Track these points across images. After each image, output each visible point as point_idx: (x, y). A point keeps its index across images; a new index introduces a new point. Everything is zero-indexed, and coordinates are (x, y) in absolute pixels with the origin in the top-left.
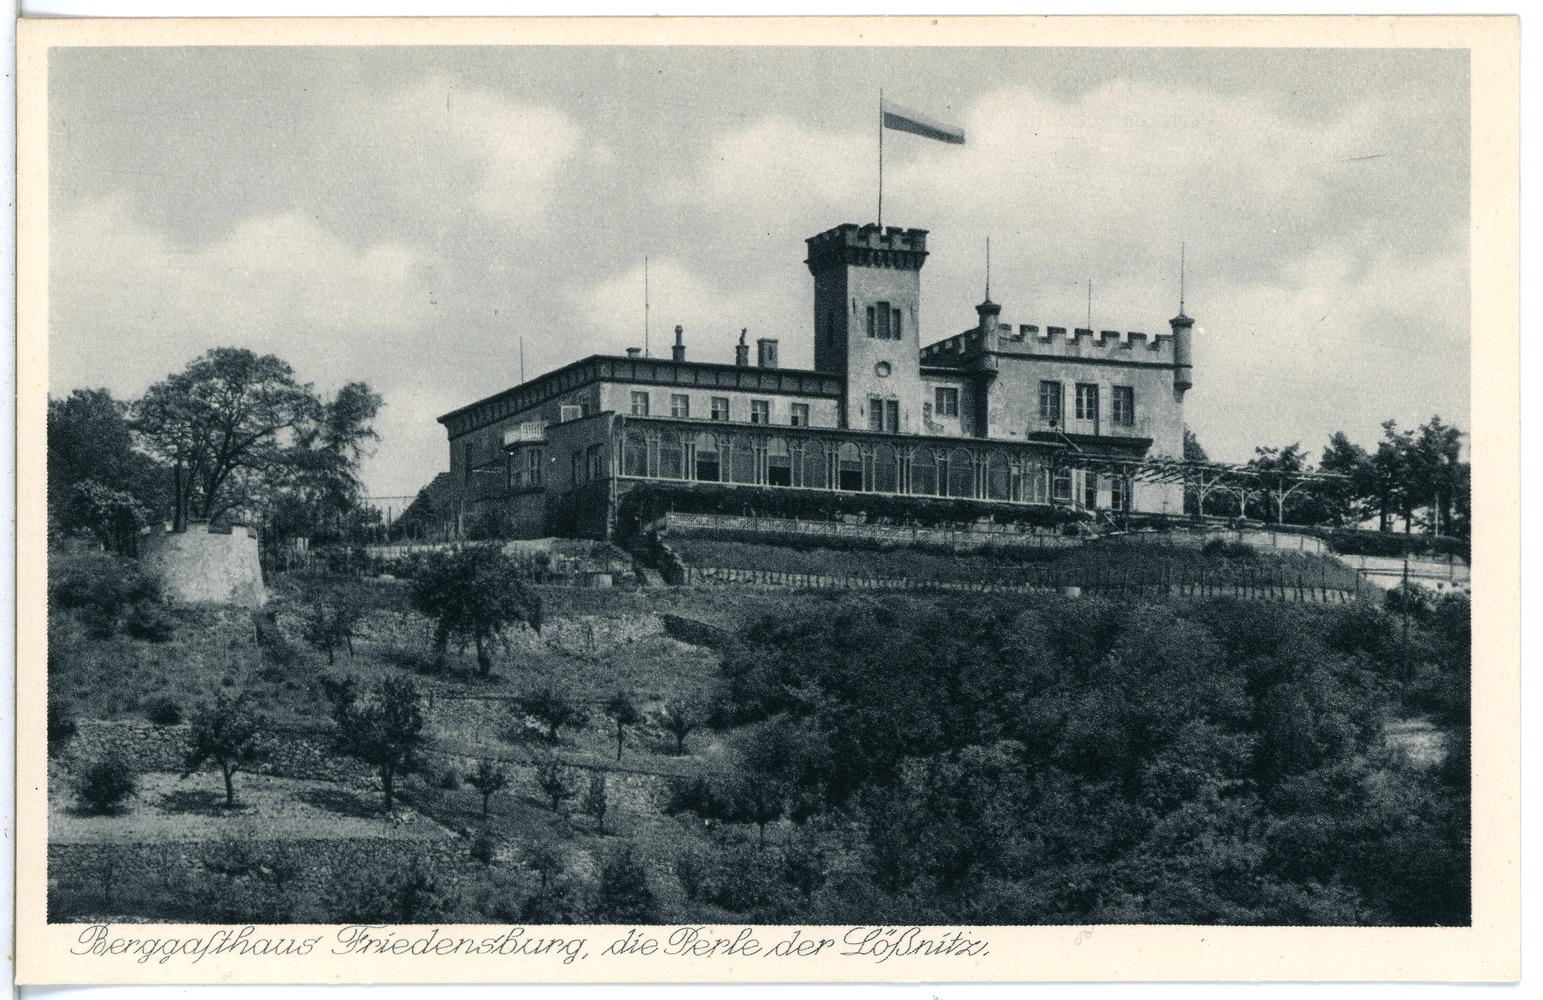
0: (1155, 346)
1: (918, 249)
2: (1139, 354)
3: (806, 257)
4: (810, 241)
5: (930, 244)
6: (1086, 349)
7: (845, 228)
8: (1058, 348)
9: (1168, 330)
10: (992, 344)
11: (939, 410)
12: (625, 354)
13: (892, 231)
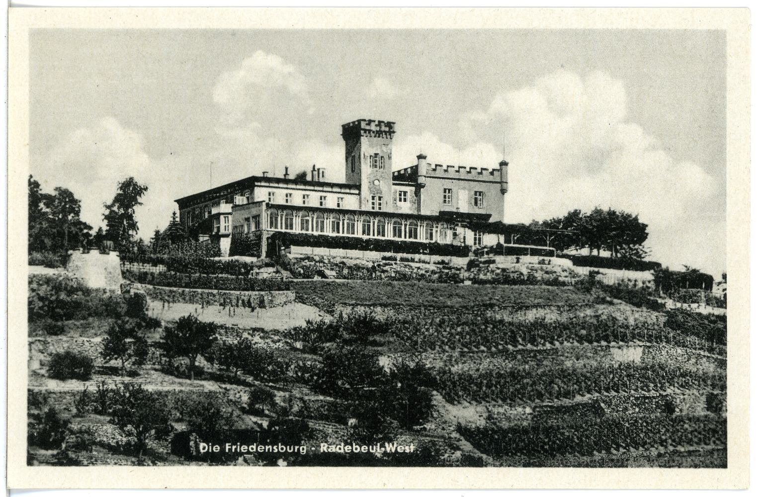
0: (492, 173)
1: (392, 130)
2: (486, 176)
3: (341, 133)
4: (343, 126)
5: (396, 128)
7: (359, 121)
8: (452, 173)
9: (498, 168)
10: (423, 171)
11: (400, 200)
12: (261, 175)
13: (380, 122)
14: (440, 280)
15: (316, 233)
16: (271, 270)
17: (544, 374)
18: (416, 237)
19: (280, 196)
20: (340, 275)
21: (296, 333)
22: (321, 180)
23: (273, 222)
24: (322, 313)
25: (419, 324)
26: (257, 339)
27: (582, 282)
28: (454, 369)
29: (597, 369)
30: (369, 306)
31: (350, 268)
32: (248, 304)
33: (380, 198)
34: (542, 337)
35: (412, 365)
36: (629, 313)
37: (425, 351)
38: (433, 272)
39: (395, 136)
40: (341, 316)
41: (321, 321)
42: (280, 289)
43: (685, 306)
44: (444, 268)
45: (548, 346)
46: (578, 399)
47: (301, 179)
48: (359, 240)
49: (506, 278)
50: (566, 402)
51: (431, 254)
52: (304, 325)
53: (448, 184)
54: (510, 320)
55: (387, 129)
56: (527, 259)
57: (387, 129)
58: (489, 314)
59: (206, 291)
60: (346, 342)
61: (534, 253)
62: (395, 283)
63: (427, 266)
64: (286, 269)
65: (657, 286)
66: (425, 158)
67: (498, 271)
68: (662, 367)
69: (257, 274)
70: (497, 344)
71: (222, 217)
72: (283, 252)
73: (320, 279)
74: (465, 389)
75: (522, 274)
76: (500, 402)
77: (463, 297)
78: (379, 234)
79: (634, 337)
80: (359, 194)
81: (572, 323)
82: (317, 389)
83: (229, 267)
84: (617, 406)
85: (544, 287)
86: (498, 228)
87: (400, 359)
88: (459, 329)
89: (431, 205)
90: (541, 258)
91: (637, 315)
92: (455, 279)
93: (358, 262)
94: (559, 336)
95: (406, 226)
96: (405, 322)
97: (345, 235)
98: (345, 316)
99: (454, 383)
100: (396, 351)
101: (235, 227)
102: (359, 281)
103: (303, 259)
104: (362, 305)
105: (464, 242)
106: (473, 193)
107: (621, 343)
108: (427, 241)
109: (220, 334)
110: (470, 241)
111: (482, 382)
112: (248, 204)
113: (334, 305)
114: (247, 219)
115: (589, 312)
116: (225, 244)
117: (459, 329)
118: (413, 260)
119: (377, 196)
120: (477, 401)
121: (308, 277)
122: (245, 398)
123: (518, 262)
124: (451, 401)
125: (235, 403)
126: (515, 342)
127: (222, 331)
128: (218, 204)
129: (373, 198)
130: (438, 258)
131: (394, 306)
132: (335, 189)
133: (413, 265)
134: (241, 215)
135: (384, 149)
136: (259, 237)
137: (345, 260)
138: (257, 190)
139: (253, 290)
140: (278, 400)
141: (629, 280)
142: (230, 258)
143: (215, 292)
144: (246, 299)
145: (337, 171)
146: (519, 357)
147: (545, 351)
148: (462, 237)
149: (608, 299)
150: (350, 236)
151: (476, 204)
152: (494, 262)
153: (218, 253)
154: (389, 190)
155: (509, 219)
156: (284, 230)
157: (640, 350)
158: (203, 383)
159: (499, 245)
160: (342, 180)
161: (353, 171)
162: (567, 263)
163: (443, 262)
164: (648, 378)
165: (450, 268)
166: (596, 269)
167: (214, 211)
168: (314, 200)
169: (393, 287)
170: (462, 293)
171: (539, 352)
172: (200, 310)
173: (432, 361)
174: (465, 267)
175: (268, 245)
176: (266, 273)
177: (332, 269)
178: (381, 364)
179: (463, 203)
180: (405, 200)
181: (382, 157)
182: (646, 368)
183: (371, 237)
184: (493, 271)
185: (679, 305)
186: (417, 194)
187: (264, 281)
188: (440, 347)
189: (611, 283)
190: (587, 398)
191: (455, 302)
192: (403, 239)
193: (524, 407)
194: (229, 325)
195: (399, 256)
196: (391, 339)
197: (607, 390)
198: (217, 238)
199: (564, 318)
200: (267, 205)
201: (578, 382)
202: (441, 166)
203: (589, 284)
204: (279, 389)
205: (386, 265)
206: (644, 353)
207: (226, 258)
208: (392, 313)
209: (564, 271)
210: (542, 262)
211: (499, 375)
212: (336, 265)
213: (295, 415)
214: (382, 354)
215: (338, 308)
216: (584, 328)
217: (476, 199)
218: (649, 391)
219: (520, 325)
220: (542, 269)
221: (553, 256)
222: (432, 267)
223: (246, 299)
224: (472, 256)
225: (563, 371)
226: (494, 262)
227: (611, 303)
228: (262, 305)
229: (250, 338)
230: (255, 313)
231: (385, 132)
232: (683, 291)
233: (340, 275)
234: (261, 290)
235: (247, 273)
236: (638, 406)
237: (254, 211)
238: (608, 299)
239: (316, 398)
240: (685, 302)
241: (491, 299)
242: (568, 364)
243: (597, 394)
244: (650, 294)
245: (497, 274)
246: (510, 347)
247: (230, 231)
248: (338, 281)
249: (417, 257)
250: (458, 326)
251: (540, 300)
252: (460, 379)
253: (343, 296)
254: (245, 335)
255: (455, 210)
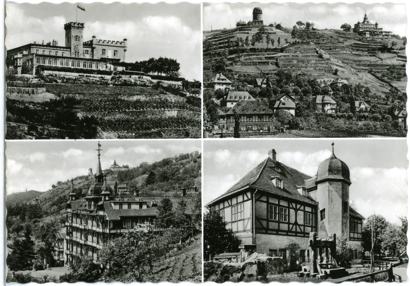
0: (121, 43)
2: (118, 44)
5: (85, 26)
6: (110, 44)
7: (71, 23)
8: (105, 43)
10: (94, 42)
13: (79, 24)
14: (101, 84)
15: (54, 66)
16: (37, 79)
17: (140, 120)
18: (92, 67)
19: (40, 52)
20: (63, 82)
21: (45, 104)
22: (56, 45)
23: (38, 61)
24: (56, 96)
25: (92, 101)
26: (31, 106)
27: (154, 86)
28: (106, 118)
29: (160, 119)
30: (74, 94)
31: (67, 79)
32: (28, 93)
33: (78, 53)
34: (139, 106)
35: (90, 116)
36: (172, 98)
37: (95, 111)
38: (98, 81)
39: (84, 29)
40: (63, 97)
41: (56, 99)
42: (40, 87)
43: (194, 95)
44: (102, 79)
45: (142, 110)
46: (153, 130)
47: (48, 45)
48: (70, 68)
49: (125, 84)
50: (149, 131)
51: (97, 74)
52: (49, 101)
53: (104, 47)
54: (127, 100)
55: (81, 26)
56: (133, 76)
57: (81, 26)
58: (119, 97)
59: (12, 87)
60: (66, 107)
61: (136, 74)
62: (84, 85)
63: (96, 79)
64: (42, 79)
65: (183, 88)
66: (95, 37)
67: (123, 81)
68: (184, 118)
69: (32, 81)
70: (122, 109)
71: (18, 60)
72: (41, 73)
73: (55, 83)
74: (109, 126)
75: (132, 82)
76: (123, 131)
77: (109, 90)
78: (78, 66)
79: (174, 107)
80: (70, 51)
81: (151, 101)
82: (53, 126)
83: (21, 79)
84: (167, 133)
85: (140, 87)
86: (123, 64)
87: (85, 114)
88: (108, 103)
89: (98, 55)
90: (139, 76)
91: (175, 98)
92: (107, 84)
93: (70, 77)
94: (146, 106)
95: (88, 64)
96: (87, 100)
97: (65, 66)
98: (65, 97)
99: (106, 124)
100: (84, 111)
101: (23, 63)
102: (70, 84)
103: (49, 76)
104: (71, 93)
105: (110, 69)
106: (113, 51)
107: (169, 109)
108: (96, 69)
109: (17, 104)
110: (112, 69)
111: (116, 123)
112: (28, 54)
113: (60, 93)
114: (28, 60)
115: (157, 97)
116: (19, 70)
117: (108, 103)
118: (90, 76)
119: (77, 52)
120: (114, 131)
121: (51, 82)
122: (26, 129)
123: (130, 77)
124: (104, 131)
125: (22, 131)
126: (129, 109)
127: (18, 103)
128: (16, 54)
129: (75, 52)
130: (100, 76)
131: (83, 94)
132: (61, 49)
133: (91, 78)
134: (25, 59)
135: (80, 33)
136: (32, 67)
137: (65, 76)
138: (32, 49)
139: (30, 87)
140: (39, 130)
141: (173, 85)
142: (21, 75)
143: (15, 88)
144: (27, 91)
145: (62, 43)
146: (130, 114)
147: (140, 112)
148: (109, 67)
149: (165, 92)
150: (67, 67)
151: (115, 55)
152: (121, 77)
153: (17, 73)
154: (81, 49)
155: (127, 61)
156: (42, 64)
157: (176, 112)
158: (10, 123)
159: (123, 70)
160: (64, 45)
161: (68, 42)
162: (149, 78)
163: (102, 77)
164: (179, 123)
165: (105, 80)
166: (160, 81)
167: (15, 57)
168: (53, 53)
169: (83, 87)
170: (109, 89)
171: (138, 112)
172: (9, 95)
173: (97, 115)
174: (110, 79)
175: (36, 70)
176: (35, 81)
177: (60, 80)
178: (78, 116)
179: (109, 54)
180: (88, 53)
181: (79, 37)
182: (178, 119)
183: (75, 67)
184: (121, 81)
185: (191, 95)
186: (92, 51)
187: (34, 84)
188: (101, 110)
189: (166, 86)
190: (156, 130)
191: (107, 92)
192: (87, 68)
193: (132, 133)
194: (20, 101)
195: (85, 75)
196: (82, 106)
197: (164, 127)
198: (16, 67)
199: (148, 99)
200: (36, 54)
201: (153, 124)
202: (101, 40)
203: (157, 86)
204: (39, 125)
205: (80, 78)
206: (178, 113)
207: (19, 75)
208: (82, 96)
209: (148, 81)
210: (139, 78)
211: (123, 121)
212: (62, 78)
213: (45, 136)
214: (78, 112)
215: (62, 94)
216: (155, 103)
217: (115, 54)
218: (179, 128)
219: (131, 102)
220: (139, 80)
221: (143, 75)
222: (98, 79)
223: (27, 91)
224: (113, 75)
225: (147, 119)
226: (121, 77)
227: (166, 94)
228: (33, 92)
229: (28, 105)
230: (30, 96)
231: (81, 27)
232: (193, 89)
233: (63, 82)
234: (33, 87)
235: (28, 81)
236: (175, 133)
237: (31, 57)
238: (165, 92)
239: (53, 129)
240: (194, 94)
241: (120, 92)
242: (149, 117)
243: (160, 129)
244: (181, 90)
245: (122, 82)
246: (127, 110)
247: (21, 64)
248: (62, 84)
249: (92, 75)
250: (107, 102)
251: (139, 92)
252: (108, 122)
253: (64, 90)
254: (27, 104)
255: (106, 57)
